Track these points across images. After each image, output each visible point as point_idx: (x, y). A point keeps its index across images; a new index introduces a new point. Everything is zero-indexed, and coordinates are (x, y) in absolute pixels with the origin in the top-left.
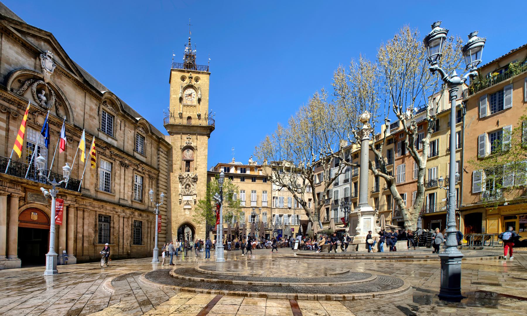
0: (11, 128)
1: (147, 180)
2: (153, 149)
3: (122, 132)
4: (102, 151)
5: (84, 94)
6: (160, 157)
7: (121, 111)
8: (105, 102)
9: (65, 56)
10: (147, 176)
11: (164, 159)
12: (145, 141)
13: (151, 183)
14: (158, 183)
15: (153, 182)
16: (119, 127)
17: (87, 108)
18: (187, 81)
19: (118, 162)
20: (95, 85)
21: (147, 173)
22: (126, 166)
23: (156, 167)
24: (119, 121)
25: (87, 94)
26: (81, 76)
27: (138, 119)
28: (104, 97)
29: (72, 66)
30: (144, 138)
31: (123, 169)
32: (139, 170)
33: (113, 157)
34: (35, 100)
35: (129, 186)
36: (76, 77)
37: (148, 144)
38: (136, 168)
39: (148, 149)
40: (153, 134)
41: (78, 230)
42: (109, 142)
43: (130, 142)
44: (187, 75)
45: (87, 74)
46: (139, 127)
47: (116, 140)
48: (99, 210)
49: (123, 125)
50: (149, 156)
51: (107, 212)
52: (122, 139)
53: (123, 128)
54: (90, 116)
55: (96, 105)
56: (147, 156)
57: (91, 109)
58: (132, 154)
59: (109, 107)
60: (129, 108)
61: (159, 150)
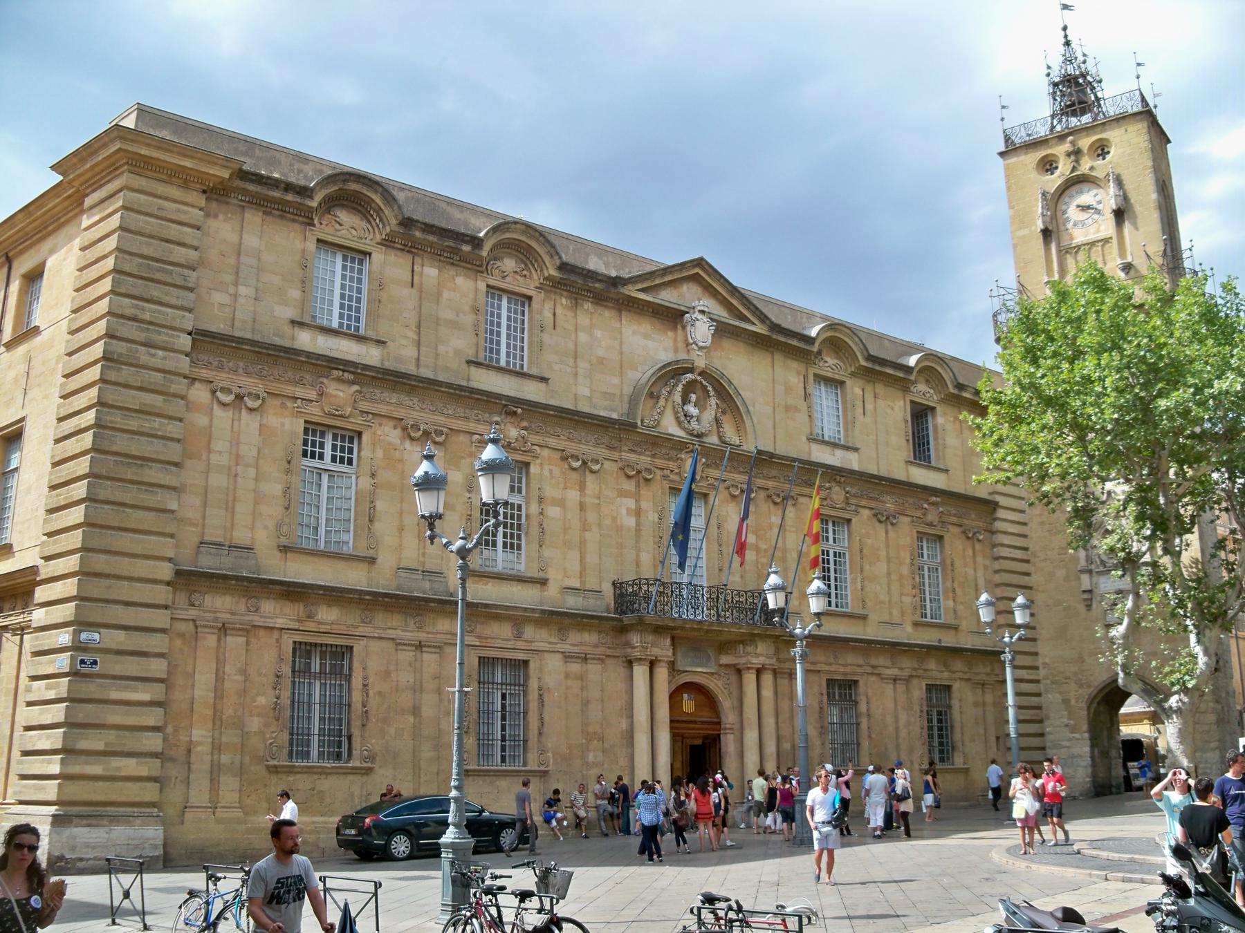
0: (644, 505)
5: (769, 359)
7: (863, 363)
8: (819, 352)
9: (728, 291)
13: (970, 552)
18: (1064, 168)
19: (866, 513)
21: (954, 520)
24: (858, 391)
26: (763, 318)
27: (912, 361)
28: (817, 345)
29: (744, 305)
31: (880, 529)
34: (679, 423)
35: (901, 577)
36: (753, 328)
37: (949, 427)
40: (960, 387)
41: (781, 733)
45: (780, 305)
46: (915, 382)
47: (856, 450)
48: (827, 668)
49: (869, 397)
50: (952, 462)
51: (848, 669)
52: (873, 437)
53: (869, 407)
54: (787, 408)
55: (798, 373)
56: (949, 466)
57: (788, 389)
59: (831, 361)
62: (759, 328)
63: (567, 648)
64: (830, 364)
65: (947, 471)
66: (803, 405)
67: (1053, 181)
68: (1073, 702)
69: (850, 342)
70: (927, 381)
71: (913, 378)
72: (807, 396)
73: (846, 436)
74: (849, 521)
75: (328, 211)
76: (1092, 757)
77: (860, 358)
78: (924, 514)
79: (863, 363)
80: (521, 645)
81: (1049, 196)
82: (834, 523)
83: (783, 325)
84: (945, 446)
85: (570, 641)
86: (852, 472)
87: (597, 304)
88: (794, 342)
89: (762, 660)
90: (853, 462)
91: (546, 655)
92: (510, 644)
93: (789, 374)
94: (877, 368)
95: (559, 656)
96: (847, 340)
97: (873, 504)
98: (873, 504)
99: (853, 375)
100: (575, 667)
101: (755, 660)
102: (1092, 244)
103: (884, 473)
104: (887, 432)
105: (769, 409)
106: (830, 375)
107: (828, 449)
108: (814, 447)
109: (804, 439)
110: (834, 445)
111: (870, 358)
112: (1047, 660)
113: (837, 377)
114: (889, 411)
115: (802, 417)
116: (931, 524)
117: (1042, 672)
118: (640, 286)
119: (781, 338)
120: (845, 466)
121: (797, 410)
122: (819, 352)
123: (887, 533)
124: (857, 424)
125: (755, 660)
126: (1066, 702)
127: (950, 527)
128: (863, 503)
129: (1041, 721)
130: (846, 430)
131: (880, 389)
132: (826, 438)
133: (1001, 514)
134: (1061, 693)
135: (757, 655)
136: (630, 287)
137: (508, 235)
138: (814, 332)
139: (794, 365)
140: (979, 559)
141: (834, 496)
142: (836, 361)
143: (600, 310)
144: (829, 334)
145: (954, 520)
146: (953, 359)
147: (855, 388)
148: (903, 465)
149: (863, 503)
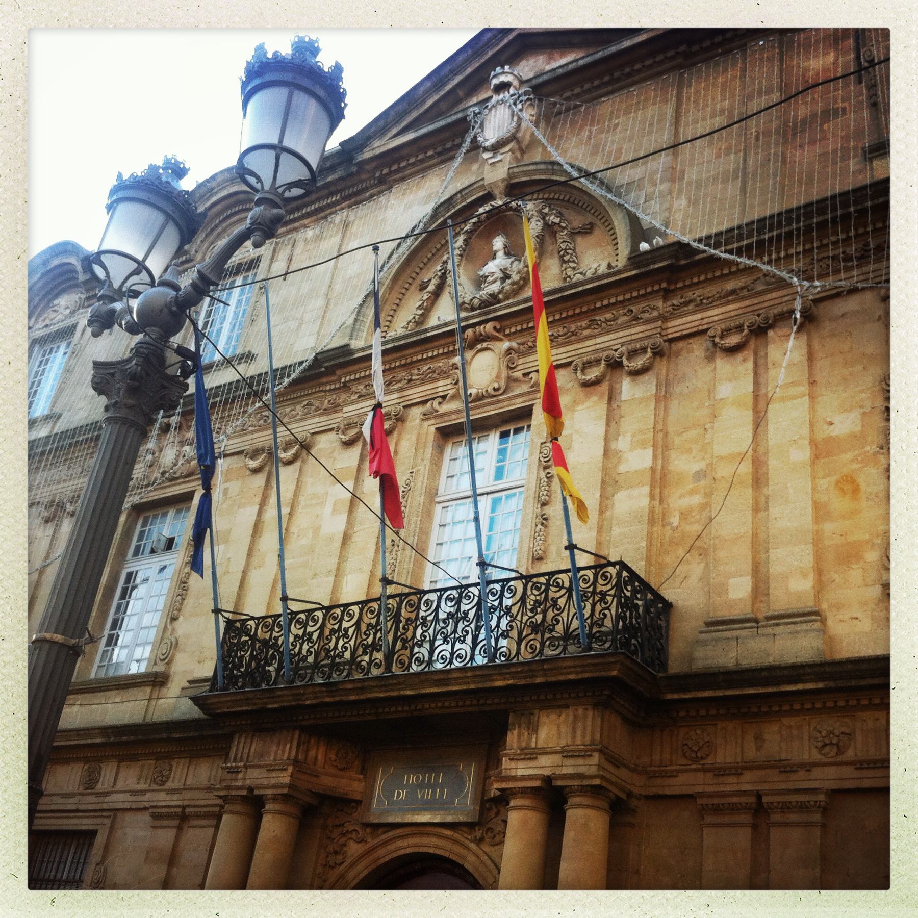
63: (162, 799)
75: (47, 306)
80: (90, 802)
85: (169, 785)
87: (357, 203)
89: (545, 765)
91: (128, 817)
92: (71, 804)
95: (146, 817)
100: (165, 837)
101: (522, 769)
118: (394, 131)
125: (522, 769)
135: (530, 754)
136: (377, 143)
137: (214, 199)
143: (362, 210)
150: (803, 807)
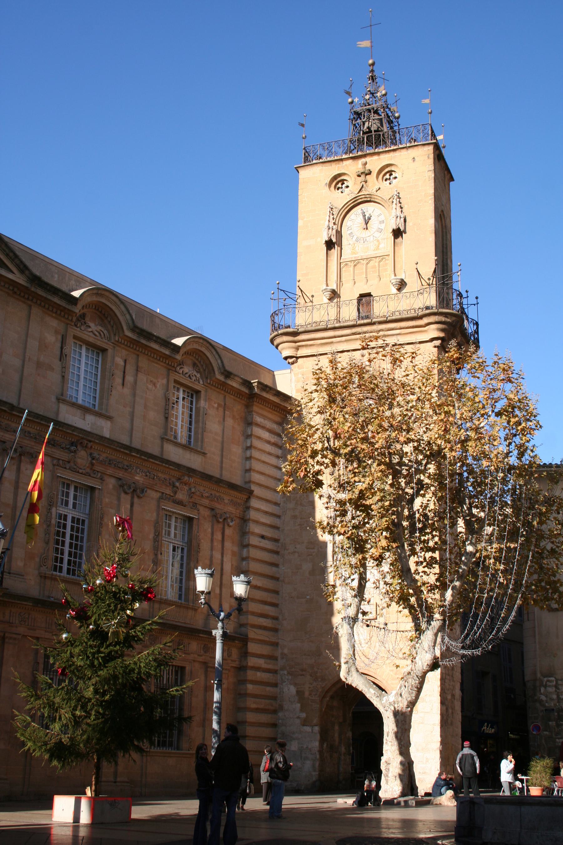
1: (207, 526)
2: (229, 422)
3: (127, 391)
4: (65, 456)
6: (257, 443)
7: (129, 334)
8: (83, 316)
10: (205, 512)
11: (268, 448)
12: (202, 403)
13: (218, 536)
14: (244, 533)
15: (228, 532)
16: (119, 380)
17: (33, 344)
18: (353, 186)
19: (111, 482)
20: (54, 281)
21: (206, 502)
22: (136, 492)
23: (237, 480)
25: (36, 311)
26: (23, 268)
27: (179, 341)
28: (79, 306)
30: (198, 392)
31: (126, 499)
32: (181, 496)
33: (97, 468)
36: (10, 276)
37: (212, 412)
38: (168, 491)
39: (213, 426)
40: (228, 375)
42: (87, 428)
43: (152, 415)
44: (351, 168)
46: (181, 364)
47: (109, 418)
49: (130, 369)
50: (212, 448)
52: (128, 409)
53: (129, 378)
54: (39, 365)
55: (57, 332)
58: (154, 450)
59: (94, 327)
60: (152, 315)
61: (249, 423)
62: (17, 277)
64: (93, 330)
65: (204, 454)
66: (57, 364)
67: (341, 198)
68: (307, 694)
69: (117, 311)
70: (194, 365)
71: (179, 357)
72: (62, 357)
73: (101, 404)
74: (92, 489)
76: (321, 752)
77: (125, 328)
78: (175, 493)
79: (129, 334)
81: (335, 212)
82: (76, 488)
83: (45, 279)
84: (204, 430)
86: (102, 438)
88: (56, 300)
90: (105, 429)
93: (46, 330)
94: (143, 341)
96: (113, 308)
97: (120, 474)
98: (120, 474)
99: (117, 344)
102: (369, 259)
103: (136, 444)
104: (146, 407)
105: (17, 362)
106: (91, 340)
107: (79, 412)
108: (63, 408)
109: (53, 399)
110: (85, 410)
111: (135, 328)
112: (286, 651)
113: (99, 343)
114: (150, 386)
115: (55, 377)
116: (180, 503)
117: (281, 663)
119: (40, 292)
120: (95, 432)
121: (50, 368)
122: (83, 316)
123: (132, 505)
124: (114, 392)
126: (300, 693)
127: (201, 509)
128: (109, 471)
129: (275, 712)
130: (101, 398)
131: (144, 362)
132: (80, 402)
133: (254, 503)
134: (295, 685)
138: (77, 294)
139: (54, 323)
140: (228, 544)
141: (79, 461)
142: (100, 328)
144: (95, 299)
145: (206, 502)
146: (225, 349)
147: (118, 358)
148: (158, 441)
149: (109, 471)
150: (15, 639)
